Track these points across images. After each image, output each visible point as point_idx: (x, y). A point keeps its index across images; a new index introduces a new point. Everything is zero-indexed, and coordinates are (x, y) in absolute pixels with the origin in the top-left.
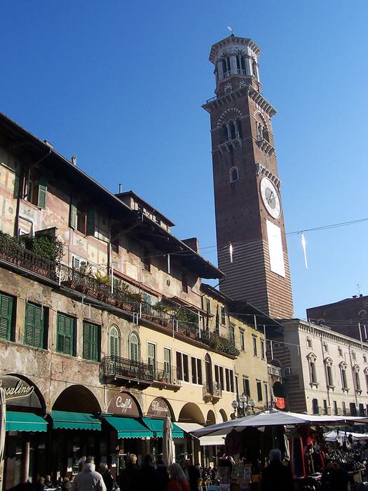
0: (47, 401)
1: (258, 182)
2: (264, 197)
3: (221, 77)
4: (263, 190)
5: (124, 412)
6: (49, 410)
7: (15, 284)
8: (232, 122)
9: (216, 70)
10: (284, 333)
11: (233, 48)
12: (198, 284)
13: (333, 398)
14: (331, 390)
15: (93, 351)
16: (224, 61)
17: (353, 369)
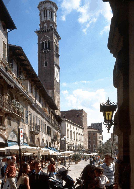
3: (43, 19)
8: (46, 42)
16: (44, 11)
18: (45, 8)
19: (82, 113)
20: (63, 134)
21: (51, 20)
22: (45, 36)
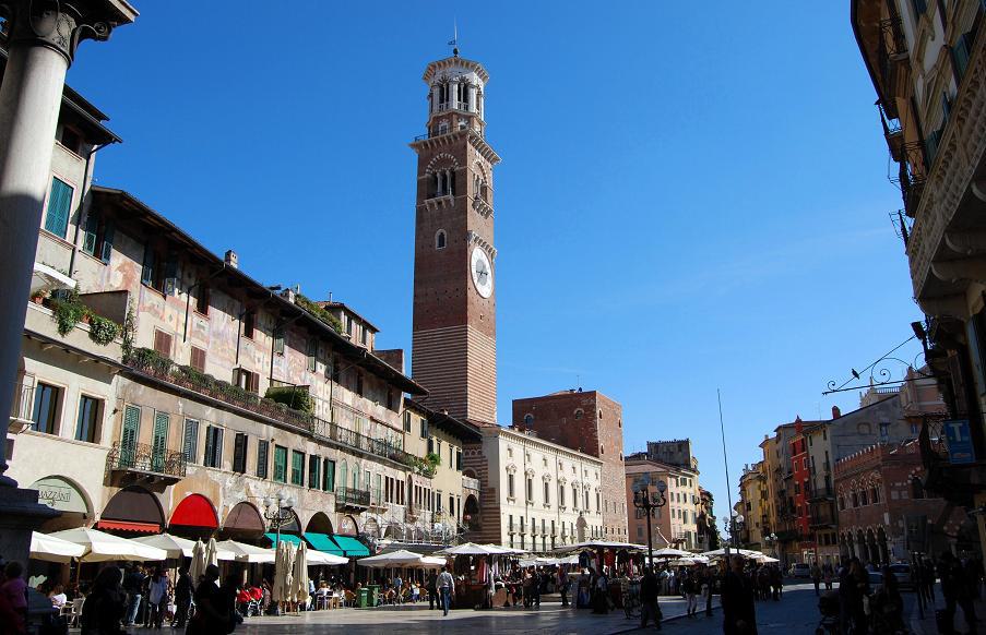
1: (469, 253)
2: (474, 271)
3: (436, 108)
4: (474, 263)
6: (303, 533)
7: (286, 437)
9: (431, 96)
14: (530, 506)
16: (441, 87)
17: (558, 481)
19: (594, 406)
20: (490, 485)
21: (462, 106)
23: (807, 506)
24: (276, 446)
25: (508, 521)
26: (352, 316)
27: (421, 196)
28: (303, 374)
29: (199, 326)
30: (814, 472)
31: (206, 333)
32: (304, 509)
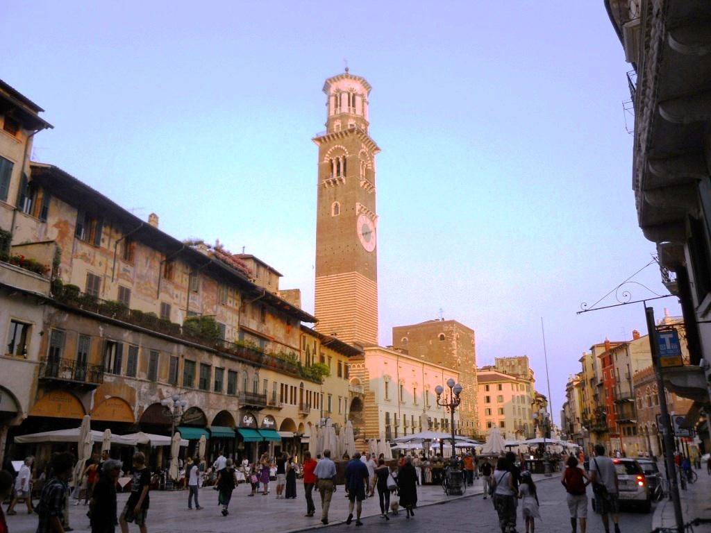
0: (209, 420)
3: (332, 113)
5: (248, 425)
6: (209, 426)
8: (338, 159)
10: (366, 356)
11: (346, 85)
12: (298, 326)
13: (403, 411)
15: (231, 390)
18: (338, 90)
20: (371, 389)
21: (352, 112)
22: (336, 146)
23: (614, 406)
24: (186, 361)
25: (384, 417)
26: (259, 263)
27: (321, 177)
28: (215, 307)
29: (125, 270)
30: (619, 382)
31: (131, 275)
32: (210, 408)
